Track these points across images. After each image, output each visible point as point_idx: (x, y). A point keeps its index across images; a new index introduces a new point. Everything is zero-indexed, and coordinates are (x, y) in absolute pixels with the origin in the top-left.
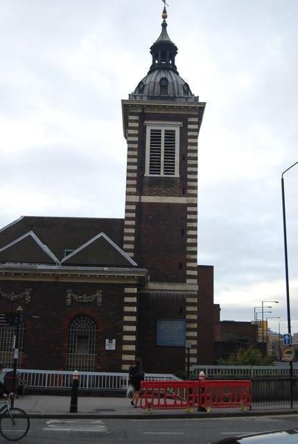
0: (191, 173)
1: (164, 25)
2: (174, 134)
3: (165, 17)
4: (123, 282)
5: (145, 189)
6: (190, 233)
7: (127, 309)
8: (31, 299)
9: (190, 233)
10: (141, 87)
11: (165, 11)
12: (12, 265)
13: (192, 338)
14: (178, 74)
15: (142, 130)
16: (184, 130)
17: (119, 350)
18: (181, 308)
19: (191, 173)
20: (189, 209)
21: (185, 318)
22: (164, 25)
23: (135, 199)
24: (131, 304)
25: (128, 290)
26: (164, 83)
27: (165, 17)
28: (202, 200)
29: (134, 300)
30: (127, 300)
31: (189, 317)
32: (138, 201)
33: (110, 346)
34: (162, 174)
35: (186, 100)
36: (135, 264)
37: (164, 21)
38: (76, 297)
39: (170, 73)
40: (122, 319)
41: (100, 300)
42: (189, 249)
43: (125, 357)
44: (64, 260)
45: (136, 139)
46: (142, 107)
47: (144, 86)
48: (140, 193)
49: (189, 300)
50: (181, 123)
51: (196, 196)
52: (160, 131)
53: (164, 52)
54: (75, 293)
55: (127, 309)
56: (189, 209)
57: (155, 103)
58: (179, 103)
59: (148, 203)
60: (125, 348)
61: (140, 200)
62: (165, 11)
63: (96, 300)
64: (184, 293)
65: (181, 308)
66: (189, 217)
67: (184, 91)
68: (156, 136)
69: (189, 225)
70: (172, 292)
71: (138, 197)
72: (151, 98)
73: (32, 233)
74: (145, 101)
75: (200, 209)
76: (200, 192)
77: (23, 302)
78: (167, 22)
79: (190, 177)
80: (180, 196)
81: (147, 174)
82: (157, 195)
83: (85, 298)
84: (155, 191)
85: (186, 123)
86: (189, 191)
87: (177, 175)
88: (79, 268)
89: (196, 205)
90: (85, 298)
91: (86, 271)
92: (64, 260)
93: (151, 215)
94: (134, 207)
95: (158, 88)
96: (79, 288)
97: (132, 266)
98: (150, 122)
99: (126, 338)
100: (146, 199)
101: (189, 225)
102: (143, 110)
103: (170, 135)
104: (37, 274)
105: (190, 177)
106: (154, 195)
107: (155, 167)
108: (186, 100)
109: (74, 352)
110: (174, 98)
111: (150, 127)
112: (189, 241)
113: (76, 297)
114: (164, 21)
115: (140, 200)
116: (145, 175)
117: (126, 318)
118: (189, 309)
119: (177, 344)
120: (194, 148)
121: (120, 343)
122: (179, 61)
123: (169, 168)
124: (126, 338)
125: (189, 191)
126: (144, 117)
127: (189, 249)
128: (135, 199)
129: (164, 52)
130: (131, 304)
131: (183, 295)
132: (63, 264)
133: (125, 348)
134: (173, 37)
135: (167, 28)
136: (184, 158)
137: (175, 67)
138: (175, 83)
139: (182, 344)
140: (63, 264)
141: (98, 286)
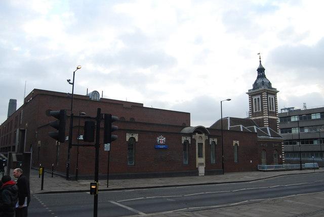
1: (260, 62)
15: (267, 96)
17: (282, 158)
22: (260, 62)
23: (267, 117)
33: (281, 157)
53: (261, 70)
68: (270, 98)
87: (274, 111)
90: (276, 145)
96: (275, 143)
99: (283, 155)
100: (270, 117)
103: (272, 98)
121: (282, 156)
122: (266, 73)
126: (268, 94)
128: (267, 117)
129: (261, 70)
134: (264, 66)
135: (261, 62)
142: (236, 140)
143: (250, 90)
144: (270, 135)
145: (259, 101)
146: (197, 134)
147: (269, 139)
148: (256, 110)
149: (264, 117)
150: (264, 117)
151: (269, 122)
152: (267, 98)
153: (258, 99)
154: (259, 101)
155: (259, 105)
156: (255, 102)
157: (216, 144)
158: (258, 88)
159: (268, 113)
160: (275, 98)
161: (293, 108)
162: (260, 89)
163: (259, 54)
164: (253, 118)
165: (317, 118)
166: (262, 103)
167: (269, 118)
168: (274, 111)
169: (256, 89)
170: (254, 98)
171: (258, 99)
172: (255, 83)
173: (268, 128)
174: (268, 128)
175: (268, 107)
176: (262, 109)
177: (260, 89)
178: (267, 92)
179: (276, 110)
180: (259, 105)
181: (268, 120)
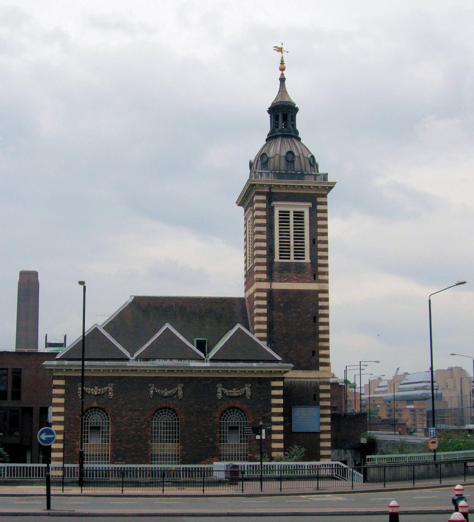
0: (322, 258)
1: (282, 80)
2: (303, 216)
3: (282, 69)
4: (269, 376)
5: (276, 274)
6: (322, 320)
7: (274, 401)
8: (183, 394)
9: (322, 320)
10: (265, 159)
11: (282, 63)
12: (168, 363)
13: (326, 424)
14: (299, 139)
15: (270, 210)
16: (313, 211)
17: (269, 440)
18: (315, 395)
19: (322, 258)
20: (320, 295)
21: (319, 405)
22: (282, 80)
23: (265, 286)
24: (277, 397)
25: (274, 384)
26: (290, 157)
27: (282, 69)
28: (331, 287)
29: (281, 392)
30: (274, 392)
31: (322, 403)
32: (269, 288)
34: (292, 260)
35: (315, 179)
36: (279, 358)
37: (282, 75)
38: (226, 391)
40: (270, 410)
41: (249, 393)
42: (321, 336)
43: (274, 445)
44: (211, 355)
45: (264, 221)
46: (270, 187)
47: (268, 159)
48: (271, 279)
49: (322, 387)
50: (310, 204)
51: (327, 282)
52: (289, 212)
54: (225, 388)
55: (274, 401)
56: (320, 295)
57: (283, 182)
58: (309, 182)
59: (278, 290)
60: (274, 437)
61: (271, 286)
62: (282, 63)
63: (245, 394)
64: (317, 380)
65: (315, 395)
66: (320, 304)
67: (311, 164)
68: (284, 215)
69: (321, 312)
70: (306, 380)
71: (269, 284)
72: (279, 176)
73: (167, 326)
74: (270, 180)
75: (331, 295)
76: (331, 277)
77: (175, 396)
78: (286, 76)
79: (320, 262)
80: (311, 282)
81: (277, 259)
82: (289, 281)
83: (235, 392)
84: (285, 277)
85: (315, 204)
86: (320, 277)
87: (307, 259)
88: (230, 364)
89: (326, 292)
90: (235, 392)
91: (237, 367)
92: (211, 355)
93: (282, 302)
94: (264, 295)
95: (283, 161)
97: (277, 361)
98: (279, 203)
99: (275, 428)
100: (277, 286)
101: (321, 312)
102: (270, 189)
103: (299, 216)
104: (191, 370)
105: (320, 262)
106: (285, 282)
107: (284, 253)
108: (315, 179)
109: (227, 442)
110: (301, 176)
111: (279, 207)
112: (321, 328)
113: (226, 391)
114: (282, 75)
115: (271, 286)
116: (275, 260)
117: (274, 410)
118: (322, 395)
119: (312, 430)
120: (323, 230)
121: (269, 432)
123: (299, 253)
124: (275, 428)
125: (320, 277)
127: (321, 336)
128: (265, 286)
130: (277, 397)
131: (316, 383)
132: (212, 360)
133: (274, 437)
135: (286, 82)
136: (314, 242)
137: (297, 132)
138: (301, 156)
139: (316, 430)
140: (212, 360)
141: (246, 380)
163: (280, 50)
167: (270, 292)
179: (314, 256)
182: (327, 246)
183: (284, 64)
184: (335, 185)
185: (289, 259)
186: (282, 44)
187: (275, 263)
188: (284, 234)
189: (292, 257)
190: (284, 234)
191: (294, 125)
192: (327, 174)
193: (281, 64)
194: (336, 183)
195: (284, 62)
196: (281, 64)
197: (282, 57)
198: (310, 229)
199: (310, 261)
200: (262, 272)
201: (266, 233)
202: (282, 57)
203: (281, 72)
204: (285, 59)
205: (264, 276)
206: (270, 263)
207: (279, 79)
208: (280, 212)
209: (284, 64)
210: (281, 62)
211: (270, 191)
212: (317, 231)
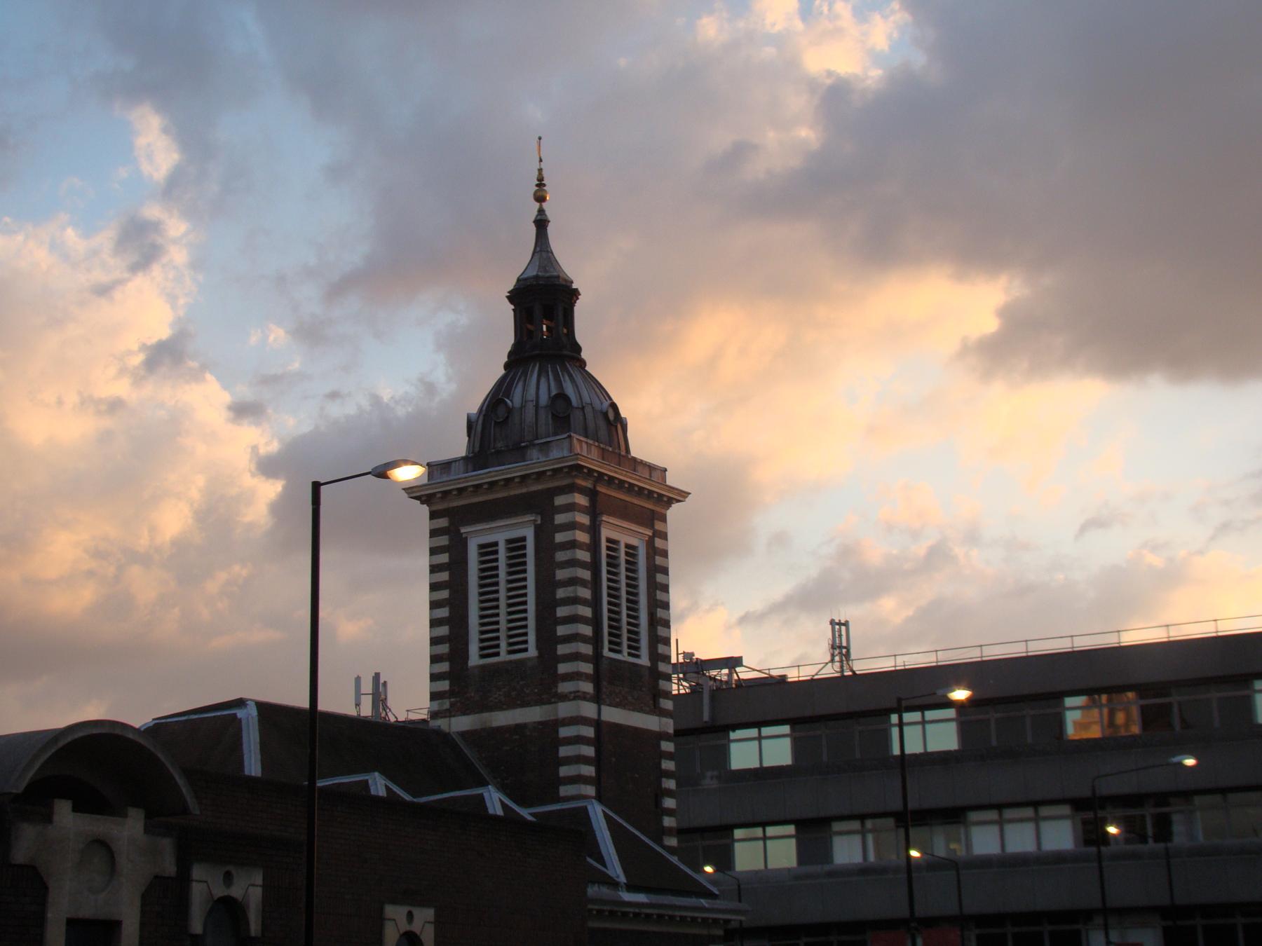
1: (541, 224)
4: (705, 932)
11: (541, 184)
15: (594, 530)
22: (541, 224)
23: (589, 710)
27: (540, 199)
32: (595, 716)
34: (624, 657)
37: (541, 211)
39: (571, 376)
48: (597, 698)
62: (541, 184)
81: (606, 652)
87: (644, 661)
94: (589, 732)
95: (602, 423)
100: (613, 715)
114: (541, 211)
128: (589, 710)
135: (551, 230)
142: (411, 897)
143: (446, 466)
144: (615, 869)
145: (517, 564)
146: (63, 811)
147: (618, 912)
148: (489, 647)
149: (565, 709)
150: (565, 709)
151: (597, 761)
152: (594, 547)
153: (516, 545)
154: (517, 564)
155: (517, 603)
156: (488, 572)
157: (255, 927)
158: (518, 451)
159: (596, 679)
160: (650, 544)
161: (733, 663)
162: (536, 461)
164: (461, 724)
165: (933, 747)
166: (546, 584)
167: (598, 724)
168: (644, 661)
169: (499, 457)
170: (477, 536)
171: (516, 545)
172: (497, 400)
173: (597, 813)
174: (597, 813)
175: (596, 622)
176: (547, 639)
177: (536, 461)
178: (592, 494)
180: (517, 603)
181: (597, 742)
182: (431, 614)
183: (544, 185)
184: (687, 500)
185: (619, 652)
186: (540, 138)
187: (604, 659)
188: (614, 593)
189: (625, 650)
190: (614, 593)
191: (574, 337)
192: (666, 470)
193: (537, 185)
194: (690, 494)
195: (543, 182)
196: (537, 185)
197: (540, 170)
198: (648, 588)
199: (649, 664)
200: (585, 677)
201: (590, 586)
202: (540, 170)
203: (537, 205)
204: (545, 173)
205: (588, 687)
206: (597, 658)
207: (534, 222)
208: (609, 540)
209: (544, 185)
210: (538, 180)
211: (595, 487)
212: (656, 595)
